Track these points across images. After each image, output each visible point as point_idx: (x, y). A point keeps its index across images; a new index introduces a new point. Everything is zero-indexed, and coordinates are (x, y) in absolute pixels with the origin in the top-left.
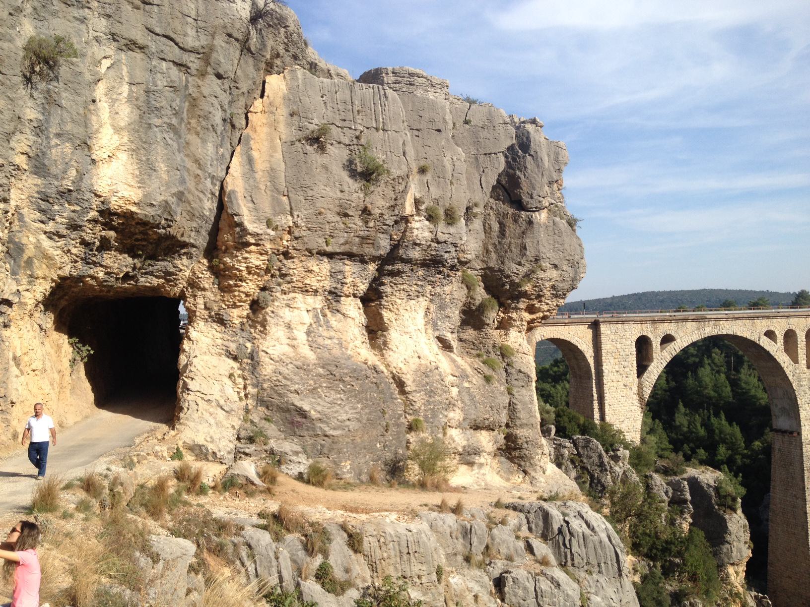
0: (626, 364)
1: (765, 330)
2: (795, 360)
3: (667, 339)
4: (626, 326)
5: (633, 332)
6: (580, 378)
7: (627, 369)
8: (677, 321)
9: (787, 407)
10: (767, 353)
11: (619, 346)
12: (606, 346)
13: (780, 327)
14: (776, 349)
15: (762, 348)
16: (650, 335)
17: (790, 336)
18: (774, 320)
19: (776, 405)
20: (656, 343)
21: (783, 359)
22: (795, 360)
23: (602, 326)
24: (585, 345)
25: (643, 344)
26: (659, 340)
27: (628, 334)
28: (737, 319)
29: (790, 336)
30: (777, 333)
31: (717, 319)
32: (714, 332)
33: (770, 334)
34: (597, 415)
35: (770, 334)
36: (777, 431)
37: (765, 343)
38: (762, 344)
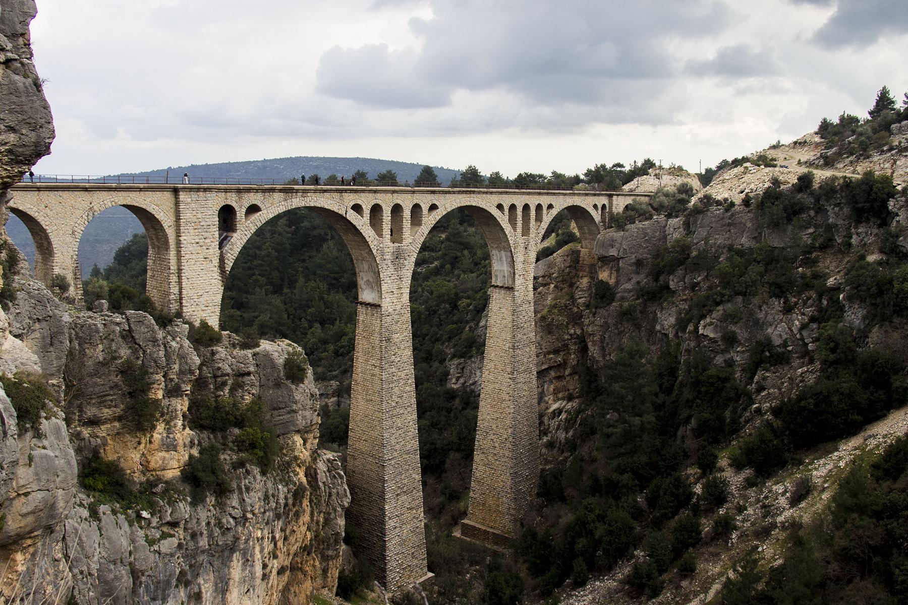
0: (206, 235)
1: (352, 203)
4: (208, 194)
5: (216, 201)
6: (159, 248)
9: (371, 280)
10: (354, 226)
11: (200, 216)
12: (186, 216)
13: (367, 202)
14: (362, 223)
15: (349, 222)
16: (234, 204)
17: (376, 210)
18: (362, 194)
20: (240, 213)
21: (368, 232)
23: (181, 193)
26: (244, 210)
27: (210, 203)
29: (376, 210)
30: (364, 207)
31: (305, 191)
32: (303, 204)
33: (357, 208)
34: (175, 290)
35: (357, 208)
36: (362, 303)
37: (352, 216)
38: (348, 218)
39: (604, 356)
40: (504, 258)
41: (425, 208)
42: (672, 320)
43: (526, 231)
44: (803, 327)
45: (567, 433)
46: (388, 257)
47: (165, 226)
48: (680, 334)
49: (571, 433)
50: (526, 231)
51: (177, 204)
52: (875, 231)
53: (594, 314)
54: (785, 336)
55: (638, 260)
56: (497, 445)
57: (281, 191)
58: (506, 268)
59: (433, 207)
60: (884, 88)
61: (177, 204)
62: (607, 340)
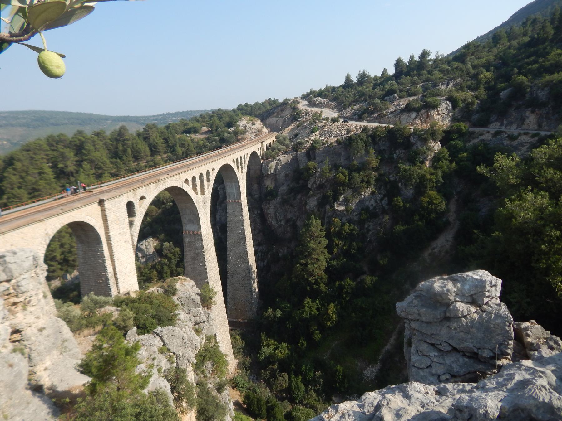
1: (184, 180)
2: (196, 193)
3: (143, 198)
7: (125, 230)
8: (146, 185)
11: (118, 215)
14: (188, 189)
19: (185, 218)
21: (191, 193)
22: (196, 193)
24: (94, 221)
25: (130, 206)
28: (173, 176)
35: (186, 181)
39: (277, 223)
40: (234, 186)
41: (210, 171)
42: (315, 203)
43: (242, 171)
44: (382, 199)
45: (264, 262)
46: (201, 204)
47: (97, 228)
48: (320, 209)
50: (242, 171)
51: (103, 211)
52: (403, 151)
53: (269, 204)
54: (374, 205)
55: (286, 174)
57: (154, 183)
58: (235, 191)
59: (213, 169)
60: (348, 74)
61: (103, 211)
62: (278, 215)
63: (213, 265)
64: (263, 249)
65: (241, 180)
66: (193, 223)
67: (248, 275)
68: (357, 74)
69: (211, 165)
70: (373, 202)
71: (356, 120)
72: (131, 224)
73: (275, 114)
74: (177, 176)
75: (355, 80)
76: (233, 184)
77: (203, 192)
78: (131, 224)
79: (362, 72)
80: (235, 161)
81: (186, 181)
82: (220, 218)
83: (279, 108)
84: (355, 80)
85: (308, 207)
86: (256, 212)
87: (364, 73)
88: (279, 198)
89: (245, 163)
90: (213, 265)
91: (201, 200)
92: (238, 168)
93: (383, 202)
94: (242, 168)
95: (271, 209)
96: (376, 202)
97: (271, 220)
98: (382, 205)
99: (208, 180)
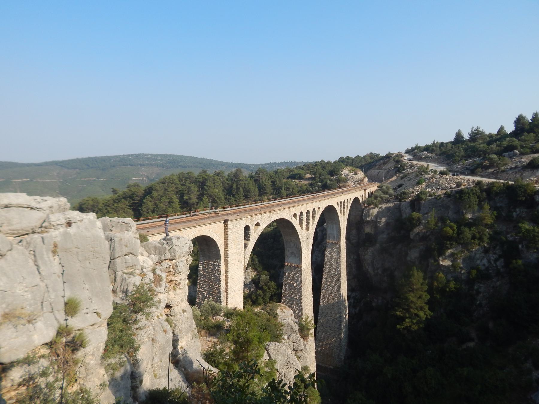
3: (258, 224)
7: (240, 250)
9: (295, 252)
14: (295, 223)
22: (302, 228)
40: (335, 227)
41: (316, 209)
42: (417, 255)
43: (344, 214)
44: (496, 260)
49: (358, 309)
50: (344, 214)
51: (226, 230)
52: (526, 210)
53: (367, 250)
54: (487, 265)
56: (331, 322)
59: (319, 208)
60: (459, 131)
61: (226, 230)
63: (309, 301)
64: (356, 296)
65: (343, 223)
66: (295, 256)
67: (339, 319)
68: (469, 131)
69: (318, 204)
70: (485, 261)
71: (468, 175)
72: (245, 246)
73: (377, 167)
74: (288, 210)
75: (466, 137)
76: (334, 226)
77: (307, 229)
78: (245, 246)
79: (474, 129)
80: (339, 203)
81: (295, 215)
82: (316, 259)
83: (382, 161)
84: (466, 137)
85: (408, 258)
86: (352, 257)
87: (477, 130)
88: (378, 246)
89: (347, 207)
90: (309, 301)
91: (305, 235)
92: (341, 211)
93: (498, 263)
94: (344, 211)
95: (368, 255)
96: (489, 261)
97: (367, 267)
98: (497, 266)
99: (314, 218)
